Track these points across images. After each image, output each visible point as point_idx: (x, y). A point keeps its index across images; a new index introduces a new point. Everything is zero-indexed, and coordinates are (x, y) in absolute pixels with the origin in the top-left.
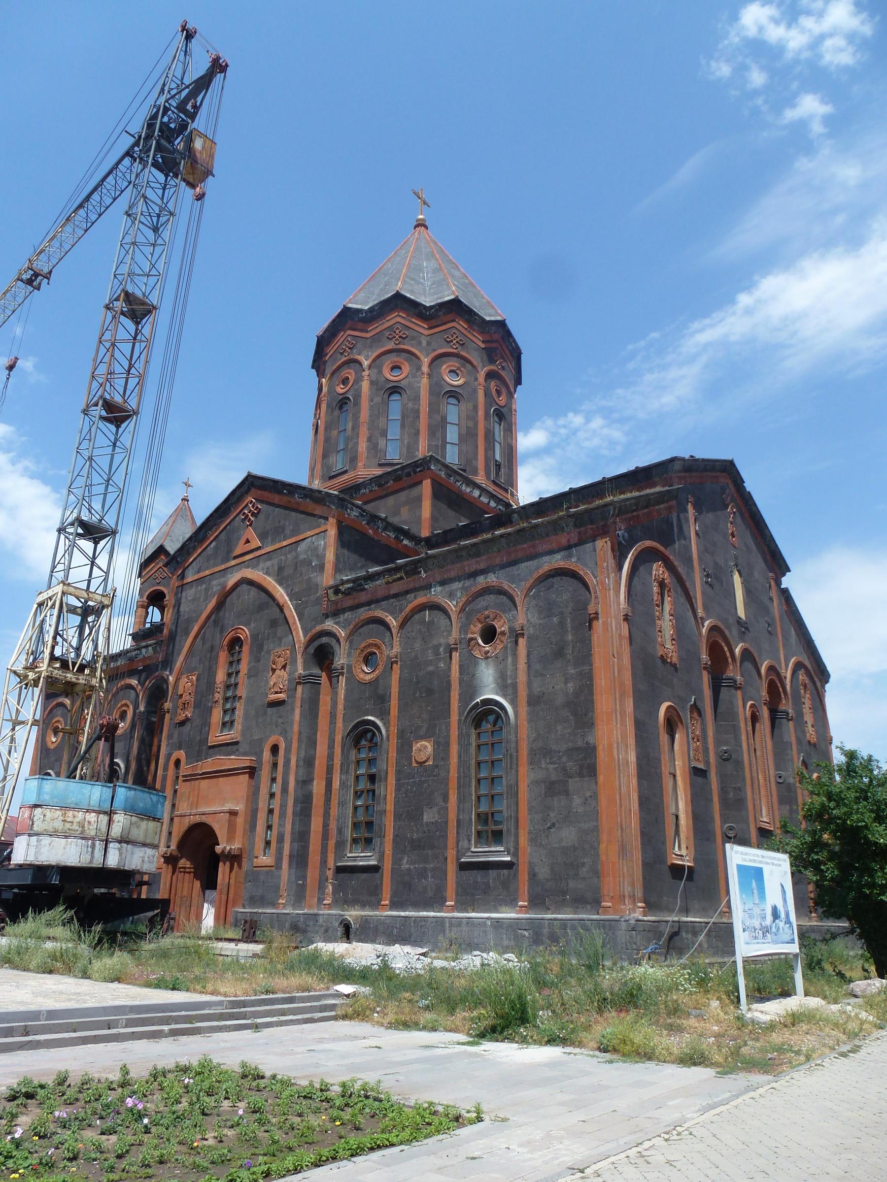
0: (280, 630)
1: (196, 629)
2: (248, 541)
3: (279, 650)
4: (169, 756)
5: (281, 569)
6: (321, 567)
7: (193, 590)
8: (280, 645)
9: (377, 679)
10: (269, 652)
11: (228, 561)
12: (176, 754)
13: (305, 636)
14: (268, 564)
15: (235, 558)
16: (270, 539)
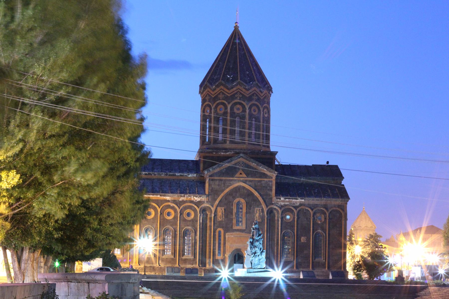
0: (257, 203)
1: (222, 195)
2: (241, 174)
3: (258, 209)
4: (216, 229)
5: (256, 186)
6: (271, 190)
7: (218, 182)
8: (258, 207)
9: (291, 222)
10: (254, 208)
11: (233, 177)
12: (219, 229)
13: (267, 206)
14: (250, 183)
15: (236, 177)
16: (250, 176)
